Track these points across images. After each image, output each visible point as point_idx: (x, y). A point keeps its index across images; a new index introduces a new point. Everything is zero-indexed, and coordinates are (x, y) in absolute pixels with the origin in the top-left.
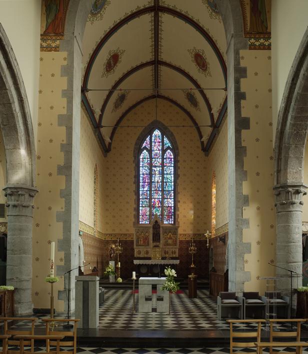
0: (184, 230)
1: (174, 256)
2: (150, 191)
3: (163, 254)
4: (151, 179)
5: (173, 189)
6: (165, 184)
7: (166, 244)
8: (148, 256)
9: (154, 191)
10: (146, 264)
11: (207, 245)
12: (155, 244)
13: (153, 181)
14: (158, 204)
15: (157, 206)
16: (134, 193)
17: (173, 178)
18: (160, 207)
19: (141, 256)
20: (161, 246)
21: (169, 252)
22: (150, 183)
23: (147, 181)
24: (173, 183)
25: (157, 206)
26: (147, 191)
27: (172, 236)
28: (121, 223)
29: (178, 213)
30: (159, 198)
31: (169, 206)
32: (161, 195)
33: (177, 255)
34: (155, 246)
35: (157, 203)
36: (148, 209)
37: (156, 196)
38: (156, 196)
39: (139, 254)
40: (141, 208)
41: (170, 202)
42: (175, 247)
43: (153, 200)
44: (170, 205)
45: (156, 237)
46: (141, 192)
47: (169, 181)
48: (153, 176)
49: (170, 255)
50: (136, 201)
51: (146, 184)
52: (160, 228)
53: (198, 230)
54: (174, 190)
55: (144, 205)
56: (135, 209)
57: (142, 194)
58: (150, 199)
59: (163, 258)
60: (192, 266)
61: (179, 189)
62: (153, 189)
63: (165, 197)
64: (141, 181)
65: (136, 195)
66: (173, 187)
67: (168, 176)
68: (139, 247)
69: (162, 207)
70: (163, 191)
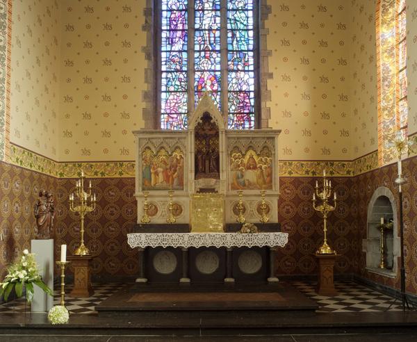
0: (288, 151)
1: (266, 219)
2: (190, 51)
3: (230, 213)
4: (191, 21)
5: (251, 47)
6: (230, 35)
7: (240, 184)
8: (180, 220)
9: (200, 51)
10: (170, 248)
11: (398, 181)
12: (203, 182)
13: (197, 26)
14: (212, 85)
15: (209, 89)
16: (143, 55)
17: (251, 21)
18: (216, 91)
19: (158, 220)
20: (223, 188)
21: (247, 205)
22: (189, 33)
23: (180, 27)
24: (251, 33)
25: (209, 89)
26: (180, 51)
27: (257, 159)
28: (106, 134)
29: (269, 104)
30: (215, 71)
31: (241, 91)
32: (220, 63)
33: (273, 217)
34: (202, 190)
35: (209, 83)
36: (184, 98)
37: (206, 65)
38: (206, 65)
39: (149, 215)
40: (163, 96)
41: (248, 80)
42: (268, 192)
43: (197, 75)
44: (244, 88)
45: (207, 163)
46: (164, 55)
47: (242, 27)
48: (198, 14)
49: (252, 215)
50: (151, 73)
51: (179, 34)
52: (217, 135)
53: (326, 151)
54: (257, 50)
55: (172, 89)
56: (146, 95)
57: (169, 60)
58: (190, 72)
59: (231, 228)
60: (325, 250)
61: (271, 43)
62: (197, 48)
63: (231, 67)
64: (164, 28)
65: (148, 57)
66: (251, 42)
67: (238, 15)
68: (151, 193)
69: (223, 92)
70: (224, 51)
